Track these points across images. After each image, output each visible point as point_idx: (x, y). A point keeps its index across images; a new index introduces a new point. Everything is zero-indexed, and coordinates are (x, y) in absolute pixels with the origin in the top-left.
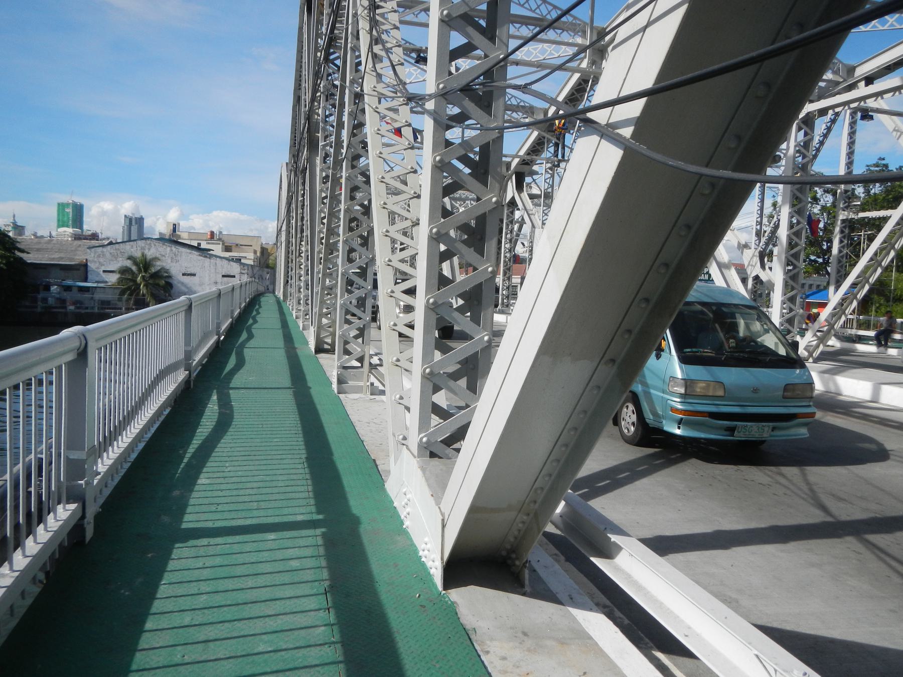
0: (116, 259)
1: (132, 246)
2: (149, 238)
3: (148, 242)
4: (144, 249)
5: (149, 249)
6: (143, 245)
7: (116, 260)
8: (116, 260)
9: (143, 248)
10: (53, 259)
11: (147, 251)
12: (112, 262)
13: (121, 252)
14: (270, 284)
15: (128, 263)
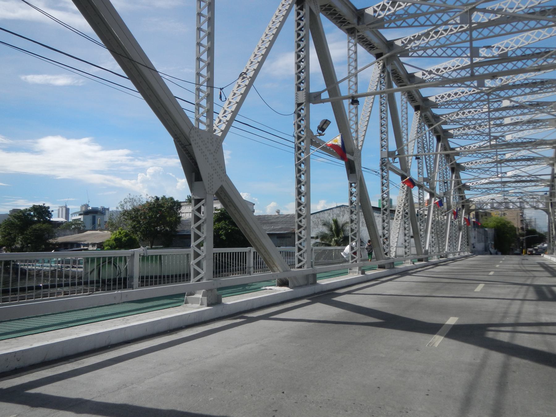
0: (318, 226)
1: (329, 214)
2: (343, 205)
3: (342, 209)
4: (339, 216)
5: (343, 216)
6: (338, 212)
7: (318, 227)
8: (318, 227)
9: (338, 215)
10: (274, 230)
11: (341, 217)
12: (314, 229)
13: (321, 220)
14: (479, 241)
15: (325, 230)
